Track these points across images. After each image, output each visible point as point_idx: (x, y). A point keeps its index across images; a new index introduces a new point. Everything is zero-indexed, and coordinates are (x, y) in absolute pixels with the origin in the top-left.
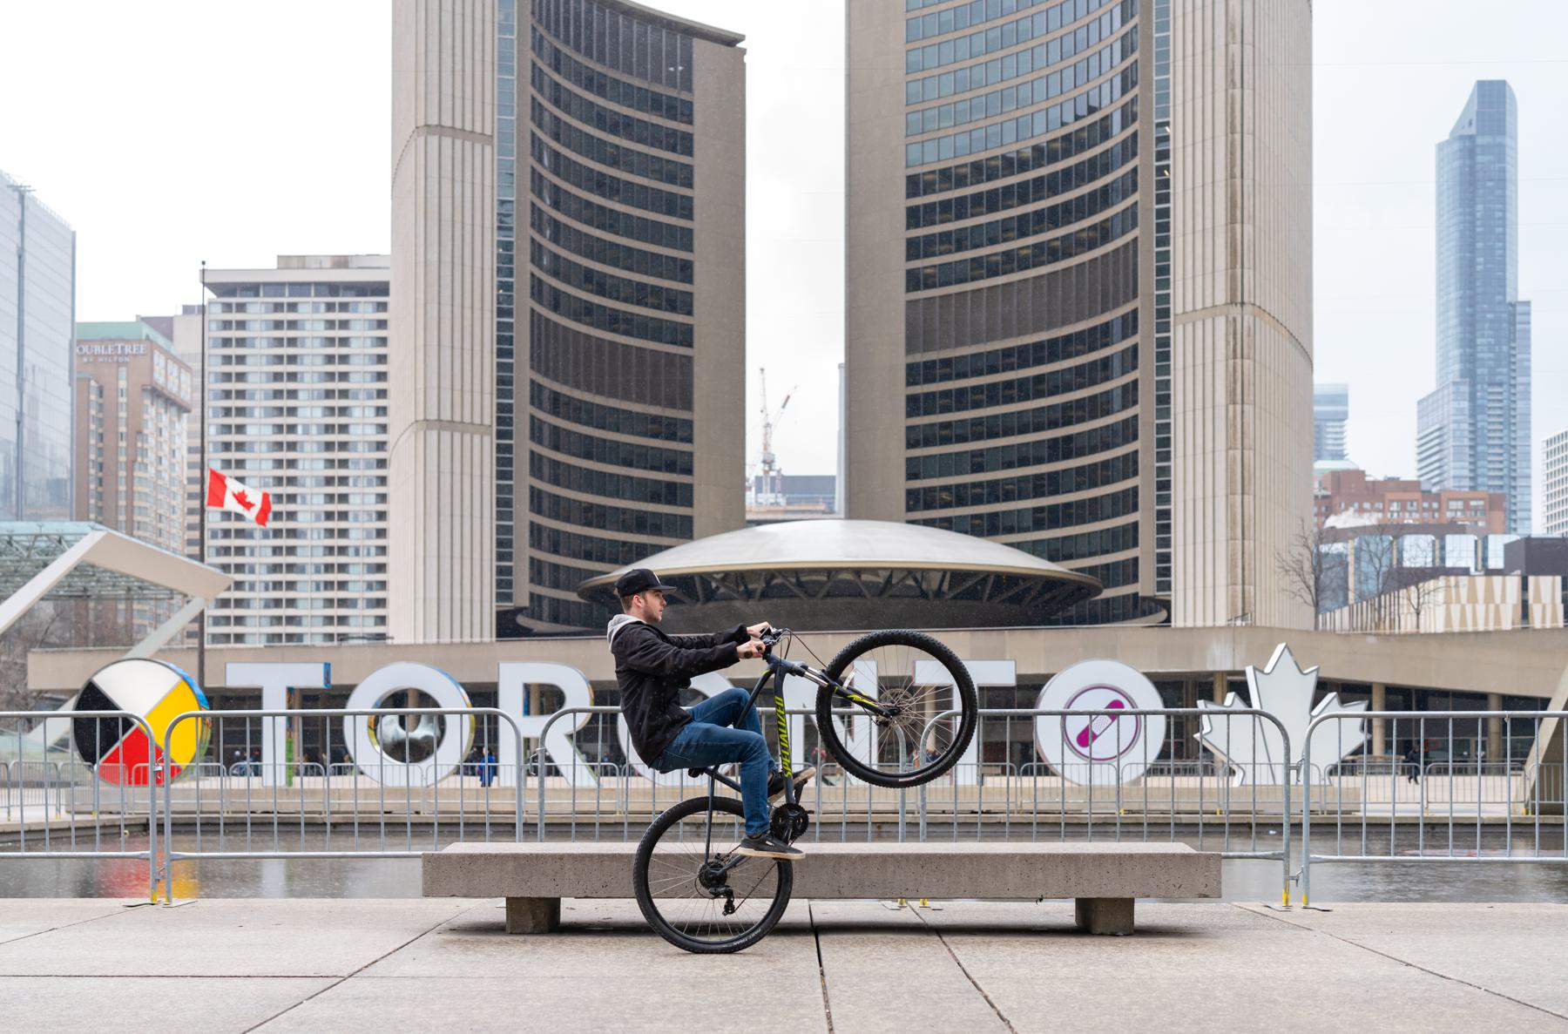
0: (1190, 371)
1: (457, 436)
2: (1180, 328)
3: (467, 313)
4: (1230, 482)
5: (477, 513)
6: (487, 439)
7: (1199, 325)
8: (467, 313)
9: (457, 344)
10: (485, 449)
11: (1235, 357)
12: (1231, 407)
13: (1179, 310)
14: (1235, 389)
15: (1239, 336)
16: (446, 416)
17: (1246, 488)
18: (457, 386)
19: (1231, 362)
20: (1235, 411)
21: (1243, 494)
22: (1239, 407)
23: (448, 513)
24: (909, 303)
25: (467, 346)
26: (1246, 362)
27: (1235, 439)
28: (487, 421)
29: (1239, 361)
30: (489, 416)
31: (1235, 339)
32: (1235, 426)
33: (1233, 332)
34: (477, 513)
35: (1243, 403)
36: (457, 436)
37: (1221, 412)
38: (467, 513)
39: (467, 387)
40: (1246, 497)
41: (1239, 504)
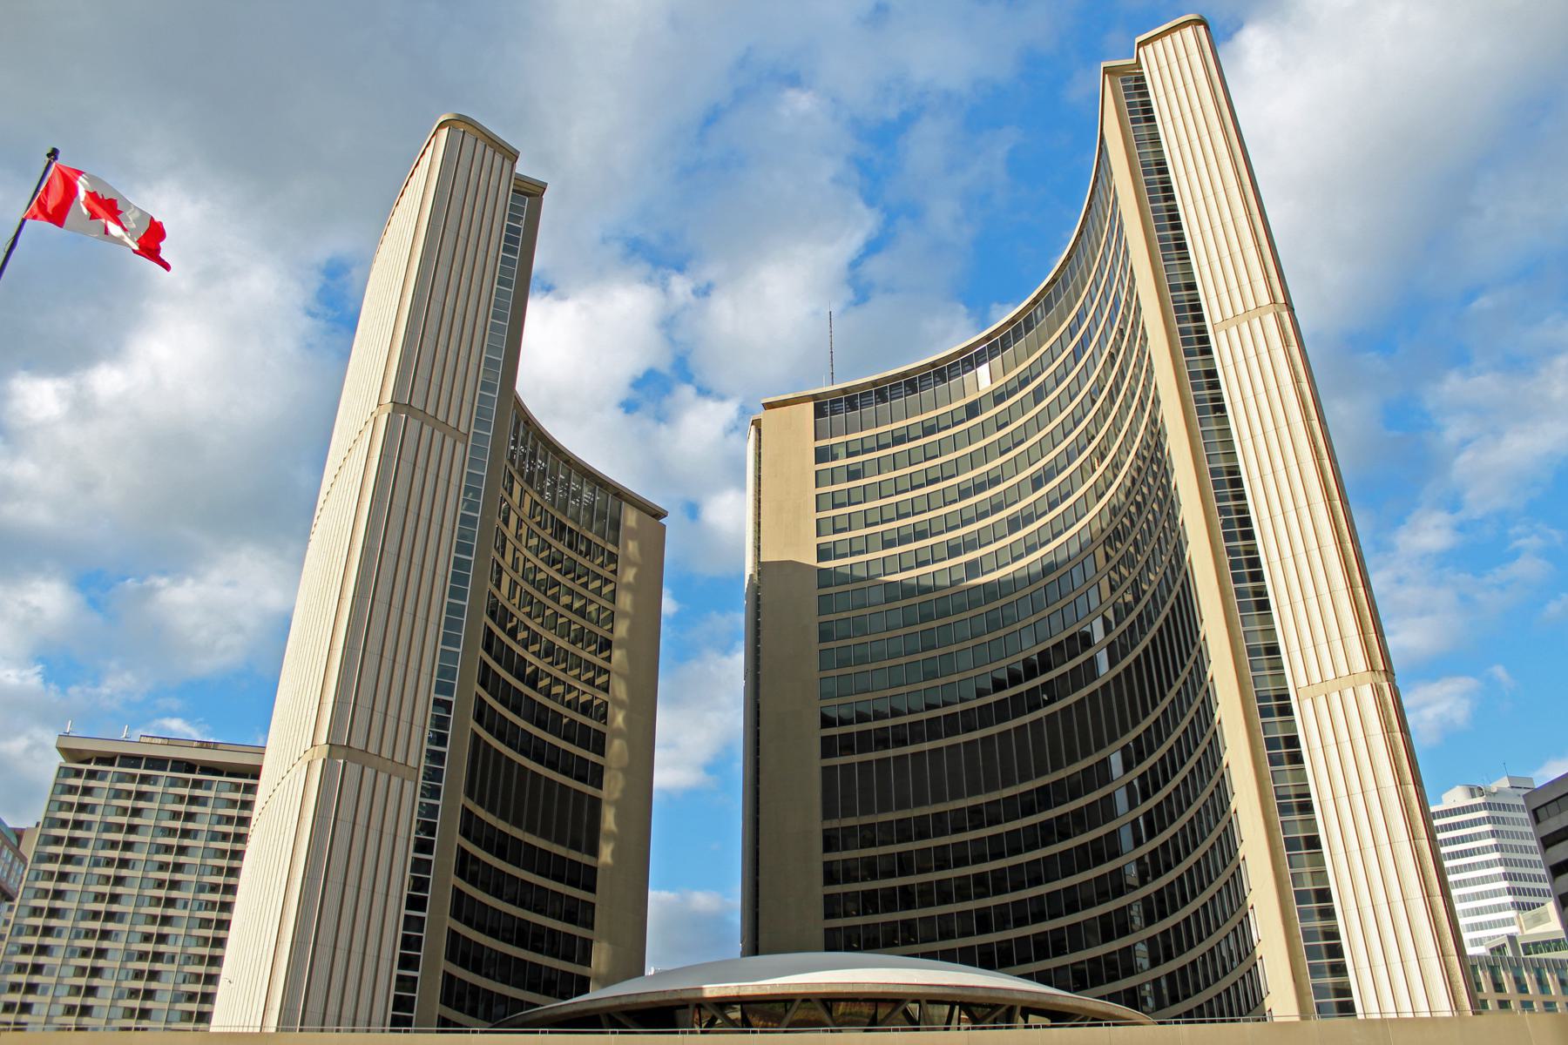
0: (1333, 751)
1: (369, 772)
2: (1308, 704)
3: (407, 619)
6: (409, 785)
7: (1335, 697)
8: (407, 619)
9: (388, 654)
10: (408, 798)
13: (1303, 682)
18: (380, 706)
23: (340, 879)
24: (824, 769)
25: (401, 659)
30: (417, 759)
36: (369, 772)
39: (392, 711)
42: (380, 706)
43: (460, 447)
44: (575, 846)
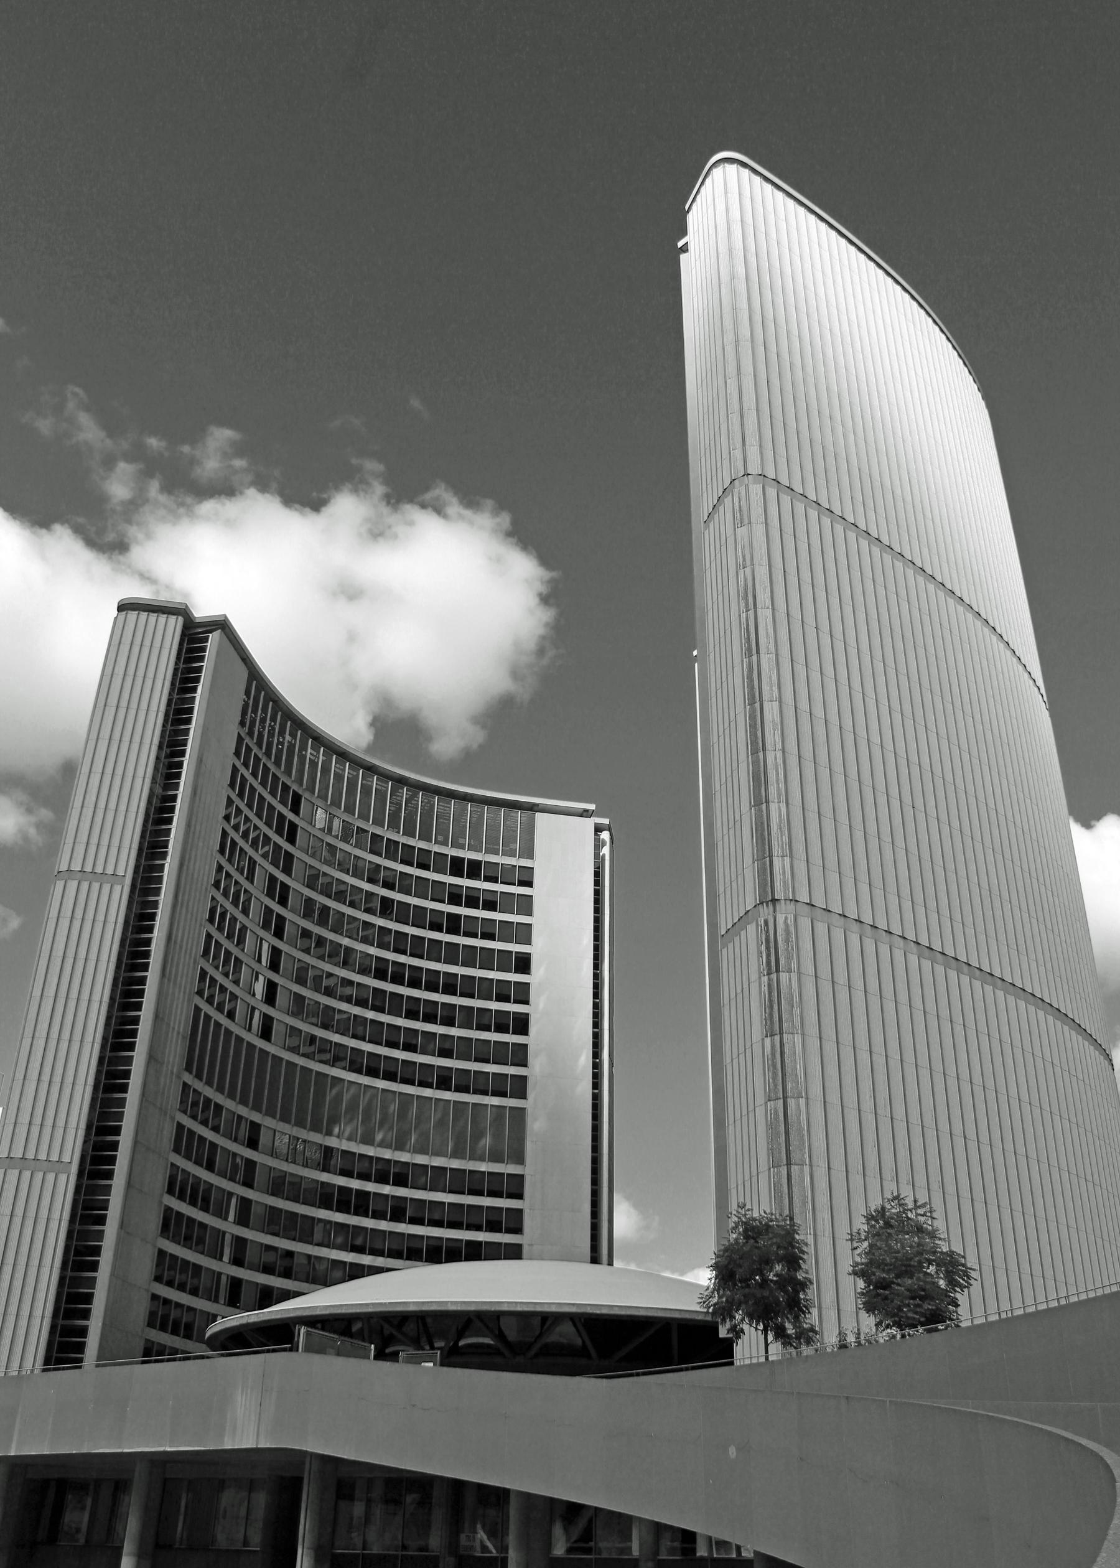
1: (27, 1174)
2: (724, 951)
4: (771, 1151)
5: (35, 1261)
6: (63, 1178)
11: (769, 974)
12: (769, 1039)
14: (771, 1015)
15: (772, 944)
16: (18, 1153)
17: (795, 1157)
18: (37, 1120)
19: (765, 979)
20: (773, 1046)
21: (789, 1164)
22: (777, 1038)
26: (783, 976)
27: (776, 1086)
28: (66, 1158)
29: (774, 976)
31: (768, 948)
32: (774, 1066)
33: (770, 944)
34: (35, 1261)
35: (781, 1033)
37: (757, 1049)
38: (22, 1261)
40: (793, 1168)
41: (785, 1181)
42: (37, 1120)
43: (117, 889)
44: (496, 1157)
